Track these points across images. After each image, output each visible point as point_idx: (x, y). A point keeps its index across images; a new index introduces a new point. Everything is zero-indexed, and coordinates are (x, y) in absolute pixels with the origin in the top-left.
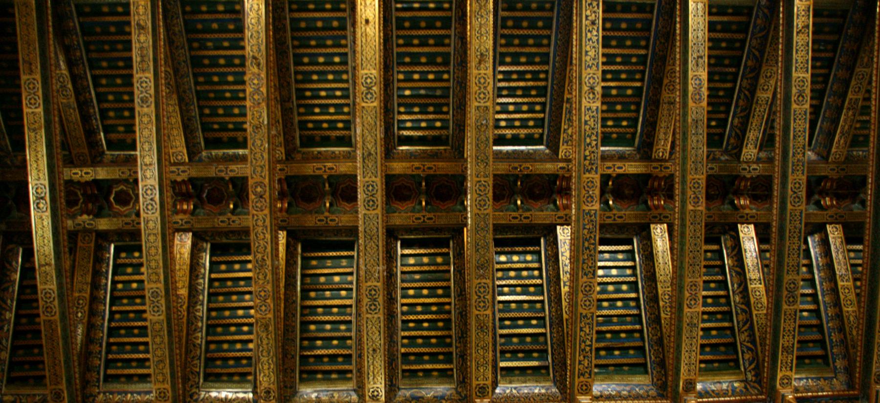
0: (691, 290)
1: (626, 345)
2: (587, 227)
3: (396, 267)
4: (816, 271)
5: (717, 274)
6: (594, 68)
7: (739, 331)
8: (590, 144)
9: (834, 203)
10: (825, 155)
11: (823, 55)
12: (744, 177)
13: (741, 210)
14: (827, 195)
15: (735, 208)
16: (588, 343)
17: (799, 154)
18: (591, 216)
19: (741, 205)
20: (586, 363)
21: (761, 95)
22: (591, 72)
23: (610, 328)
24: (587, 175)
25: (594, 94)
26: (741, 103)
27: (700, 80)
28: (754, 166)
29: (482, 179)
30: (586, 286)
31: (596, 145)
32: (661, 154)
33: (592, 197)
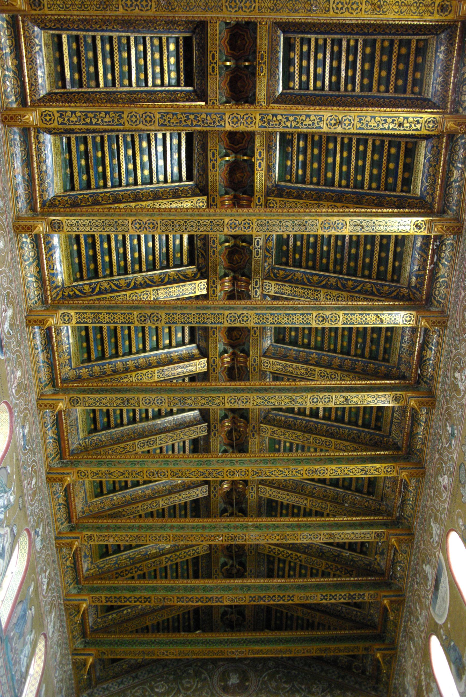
0: (149, 224)
1: (91, 171)
2: (209, 118)
4: (166, 351)
5: (161, 263)
6: (359, 125)
8: (288, 120)
10: (267, 354)
11: (353, 346)
12: (249, 284)
13: (220, 282)
14: (232, 360)
15: (222, 278)
16: (94, 121)
18: (219, 121)
19: (224, 283)
20: (74, 119)
21: (322, 294)
22: (356, 122)
24: (258, 117)
25: (335, 124)
26: (315, 278)
27: (342, 228)
28: (259, 292)
29: (257, 4)
30: (150, 117)
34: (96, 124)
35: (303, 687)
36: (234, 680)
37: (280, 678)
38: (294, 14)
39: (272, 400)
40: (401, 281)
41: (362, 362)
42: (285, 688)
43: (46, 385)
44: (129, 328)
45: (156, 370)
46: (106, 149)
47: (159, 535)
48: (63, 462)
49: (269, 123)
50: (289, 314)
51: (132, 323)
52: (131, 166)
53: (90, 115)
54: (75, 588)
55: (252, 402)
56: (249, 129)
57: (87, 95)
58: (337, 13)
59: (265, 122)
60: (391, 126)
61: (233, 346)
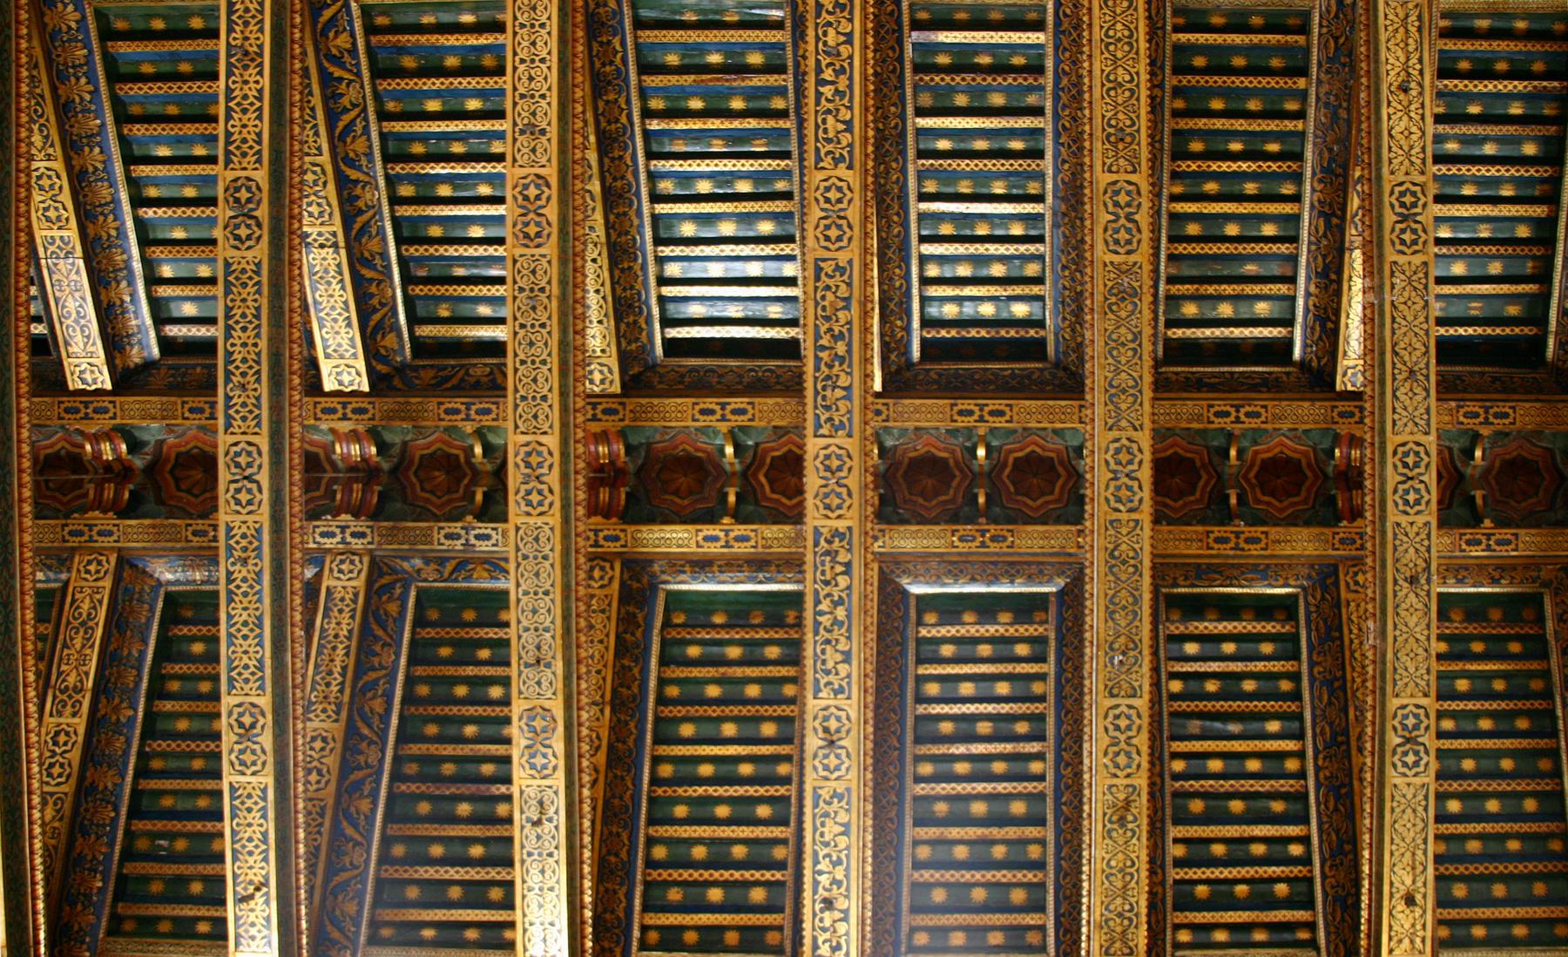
3: (1308, 294)
4: (137, 266)
5: (421, 260)
6: (826, 794)
7: (364, 110)
8: (836, 604)
9: (88, 447)
12: (356, 515)
13: (361, 428)
14: (108, 467)
15: (374, 435)
16: (827, 91)
17: (245, 580)
18: (830, 419)
20: (832, 38)
21: (327, 725)
22: (834, 784)
23: (736, 124)
24: (841, 525)
25: (826, 730)
26: (378, 705)
28: (329, 543)
31: (817, 602)
32: (597, 573)
34: (819, 95)
38: (1102, 608)
44: (212, 160)
46: (752, 123)
49: (828, 553)
51: (228, 162)
52: (704, 187)
53: (843, 83)
56: (810, 502)
58: (1106, 717)
59: (829, 542)
60: (824, 880)
61: (152, 469)
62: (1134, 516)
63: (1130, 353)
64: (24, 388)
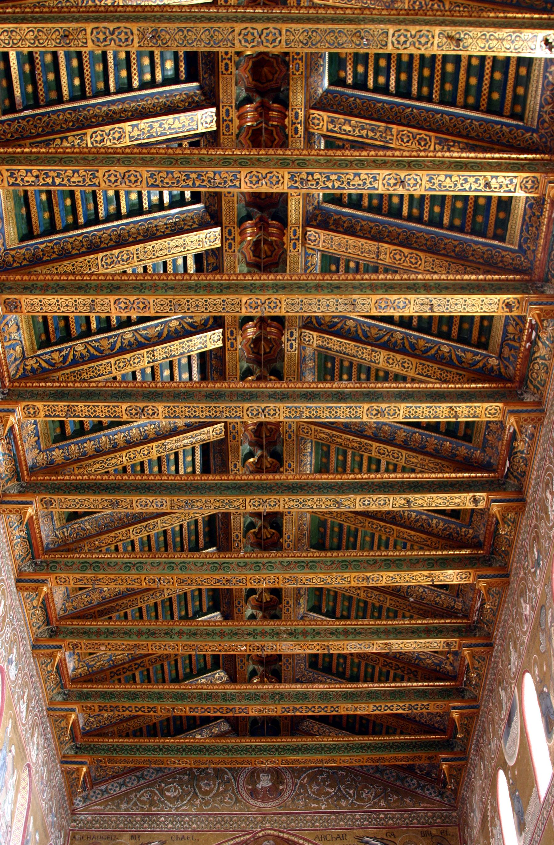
2: (217, 177)
6: (429, 185)
8: (328, 179)
16: (58, 181)
18: (231, 181)
19: (246, 329)
24: (287, 176)
25: (395, 185)
27: (404, 307)
28: (295, 345)
29: (284, 38)
30: (136, 176)
31: (328, 188)
33: (257, 182)
35: (351, 792)
36: (265, 782)
37: (324, 780)
39: (310, 503)
40: (490, 348)
41: (436, 438)
42: (329, 793)
43: (9, 480)
45: (154, 445)
47: (164, 643)
48: (36, 564)
50: (331, 407)
54: (59, 693)
55: (282, 505)
57: (45, 119)
59: (296, 182)
62: (284, 32)
63: (190, 33)
64: (225, 477)
